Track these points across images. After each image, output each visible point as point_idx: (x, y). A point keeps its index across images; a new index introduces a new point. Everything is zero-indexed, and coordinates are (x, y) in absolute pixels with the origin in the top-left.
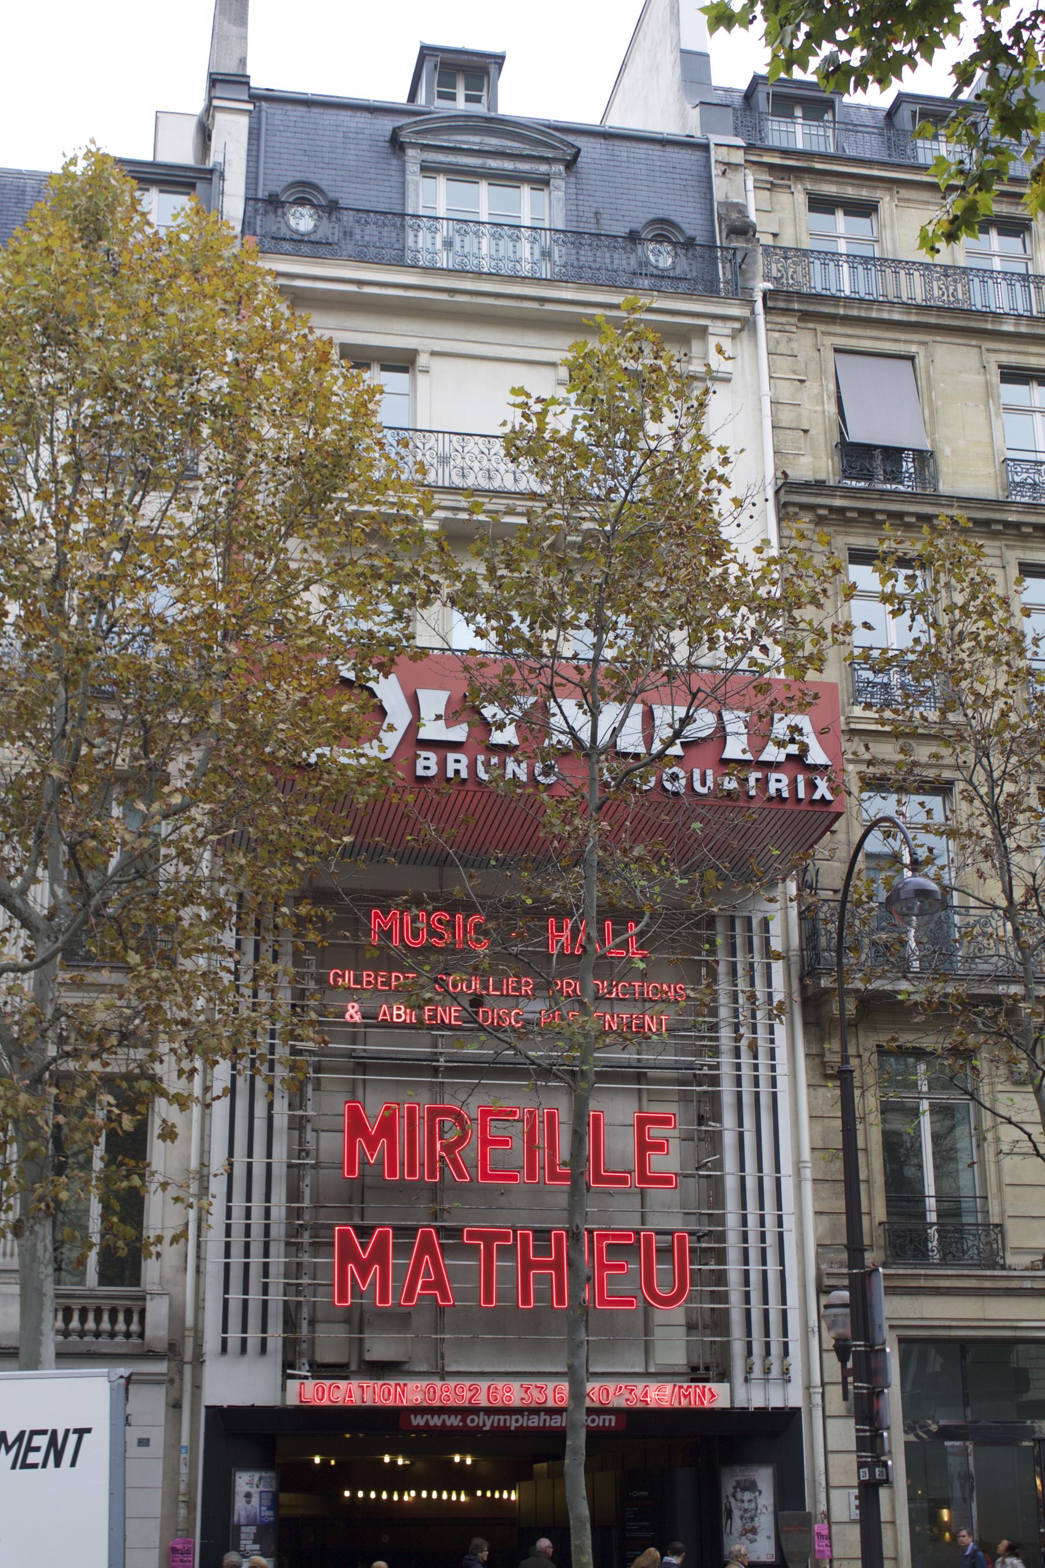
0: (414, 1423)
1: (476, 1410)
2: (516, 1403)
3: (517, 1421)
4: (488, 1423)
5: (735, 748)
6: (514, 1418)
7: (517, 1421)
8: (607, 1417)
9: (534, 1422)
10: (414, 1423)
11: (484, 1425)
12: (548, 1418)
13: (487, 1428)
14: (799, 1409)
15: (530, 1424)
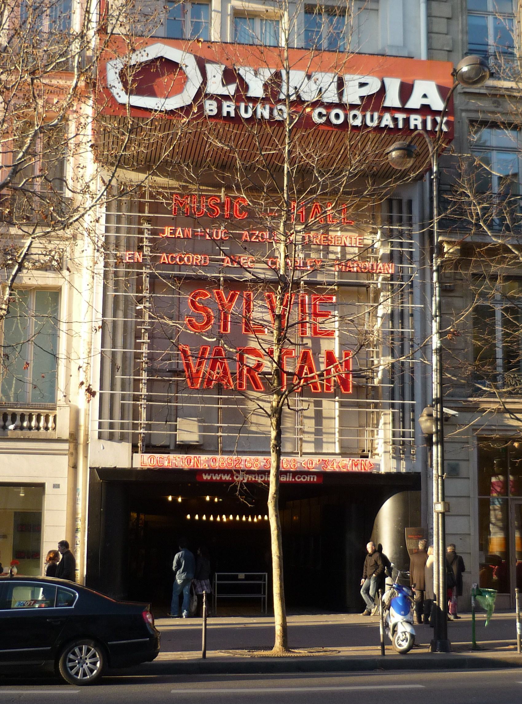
5: (392, 99)
8: (312, 476)
14: (420, 473)
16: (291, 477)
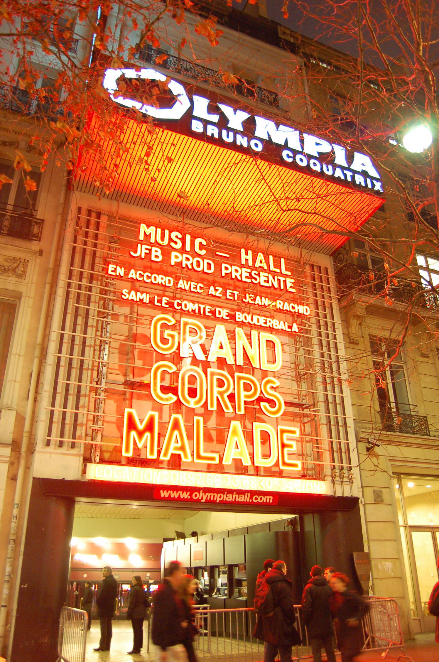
15: (228, 500)
16: (249, 498)
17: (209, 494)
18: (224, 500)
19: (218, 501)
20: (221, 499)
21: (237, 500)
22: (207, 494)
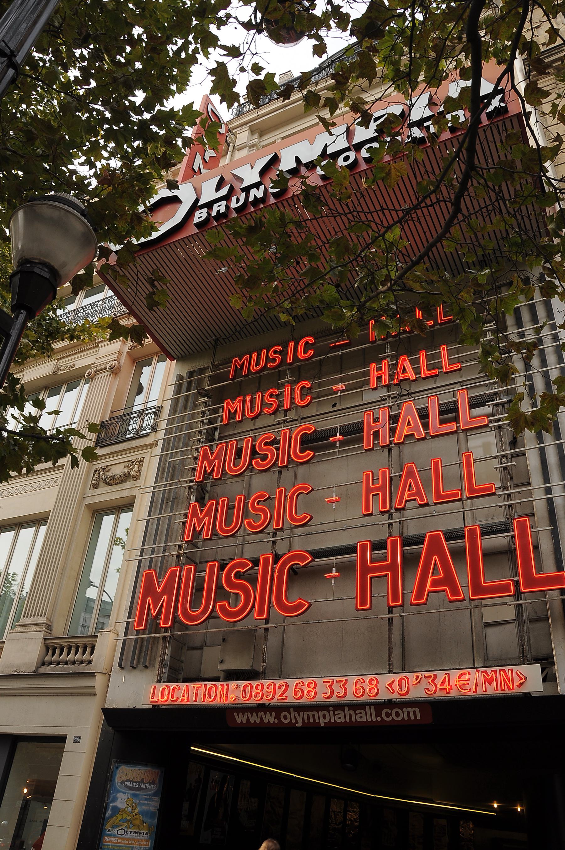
0: (239, 721)
1: (287, 708)
2: (320, 699)
3: (324, 717)
4: (300, 720)
6: (321, 713)
7: (324, 717)
9: (340, 718)
10: (239, 721)
11: (297, 722)
12: (352, 712)
13: (299, 725)
17: (306, 714)
18: (333, 721)
19: (322, 725)
20: (326, 721)
21: (354, 720)
22: (301, 713)
